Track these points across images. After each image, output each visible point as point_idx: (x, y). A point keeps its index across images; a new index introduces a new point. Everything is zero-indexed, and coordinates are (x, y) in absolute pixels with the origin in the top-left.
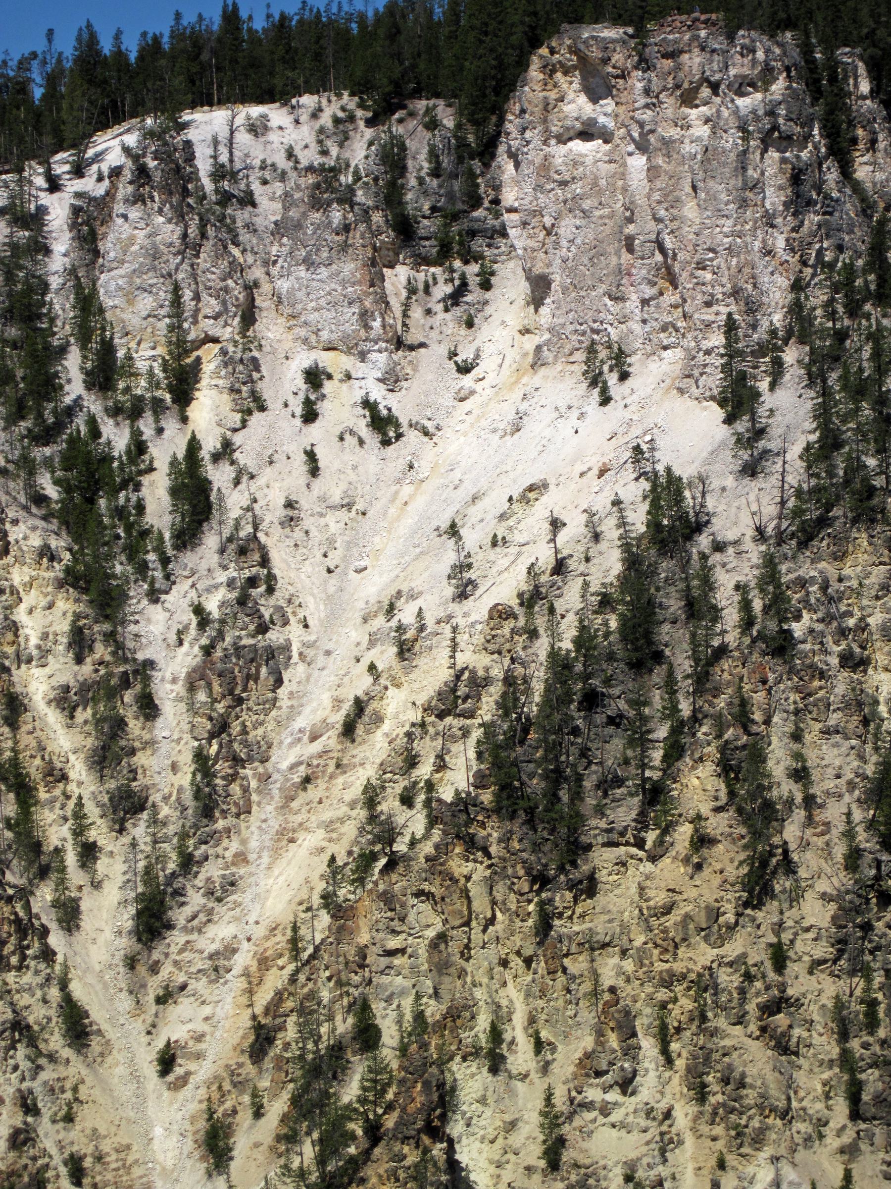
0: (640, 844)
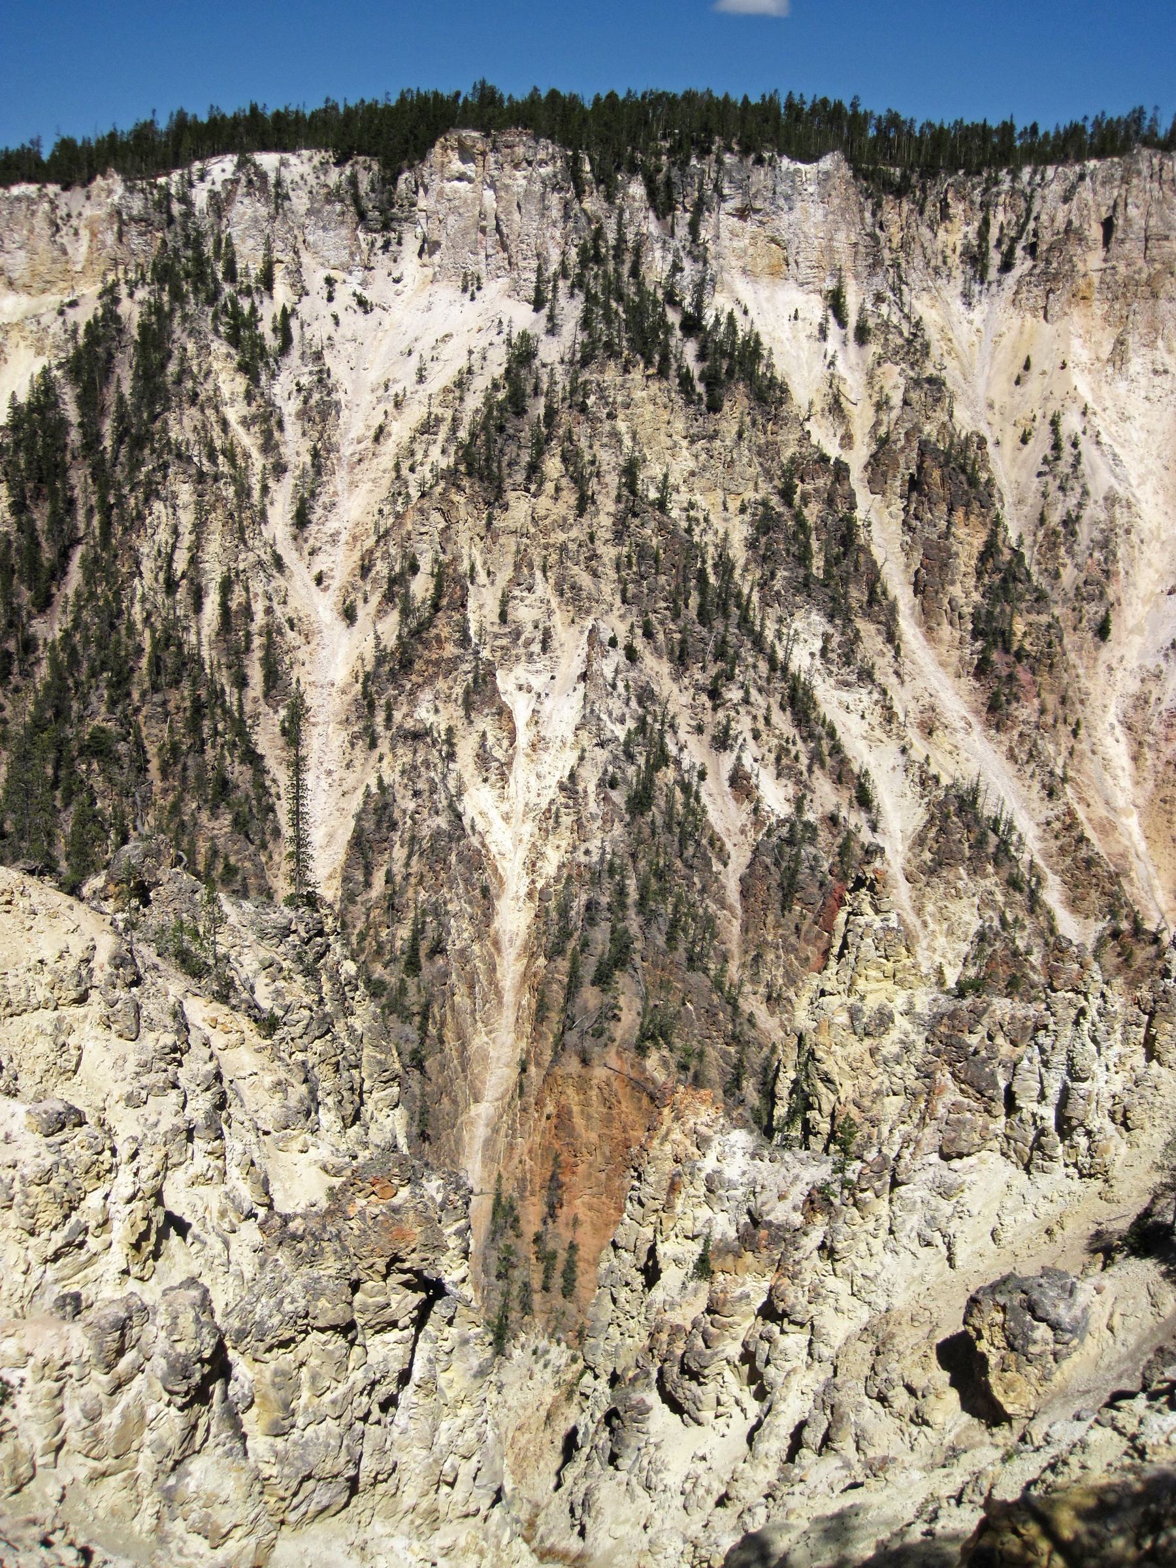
0: (527, 490)
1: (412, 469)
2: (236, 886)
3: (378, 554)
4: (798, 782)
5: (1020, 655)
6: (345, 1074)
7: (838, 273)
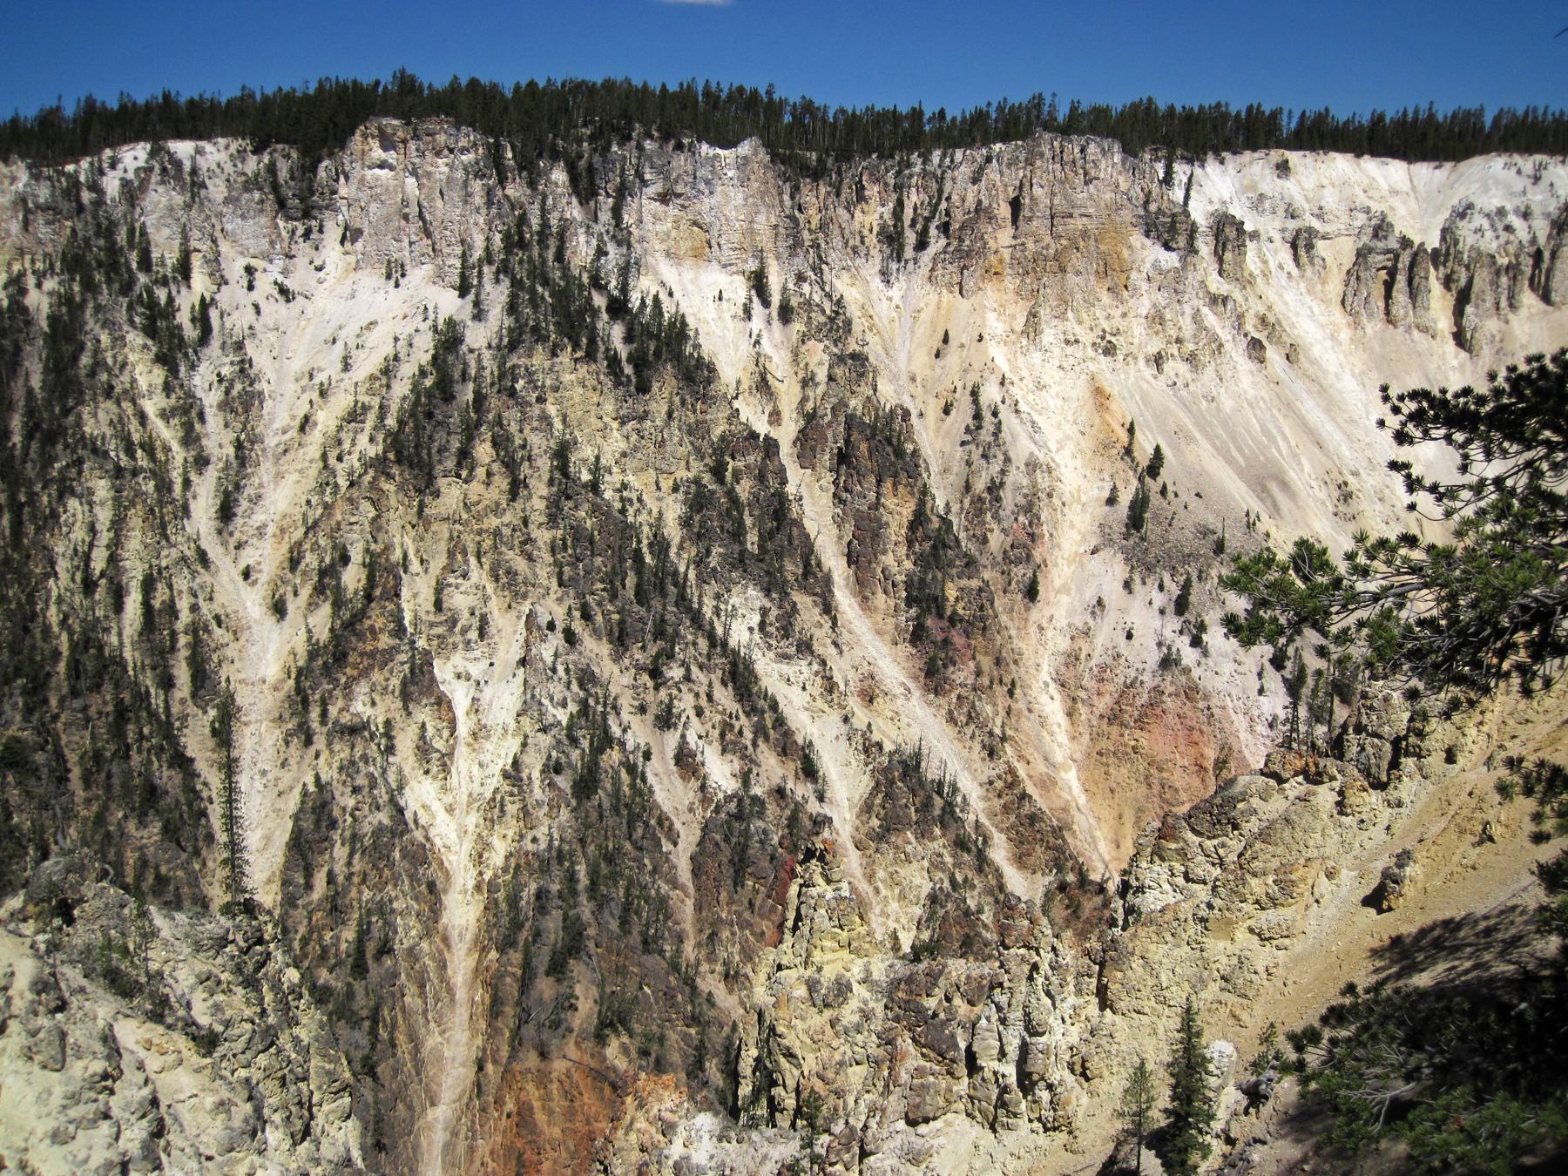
0: (458, 476)
1: (340, 459)
2: (169, 897)
3: (307, 546)
4: (743, 757)
5: (953, 620)
6: (293, 1088)
7: (760, 254)
